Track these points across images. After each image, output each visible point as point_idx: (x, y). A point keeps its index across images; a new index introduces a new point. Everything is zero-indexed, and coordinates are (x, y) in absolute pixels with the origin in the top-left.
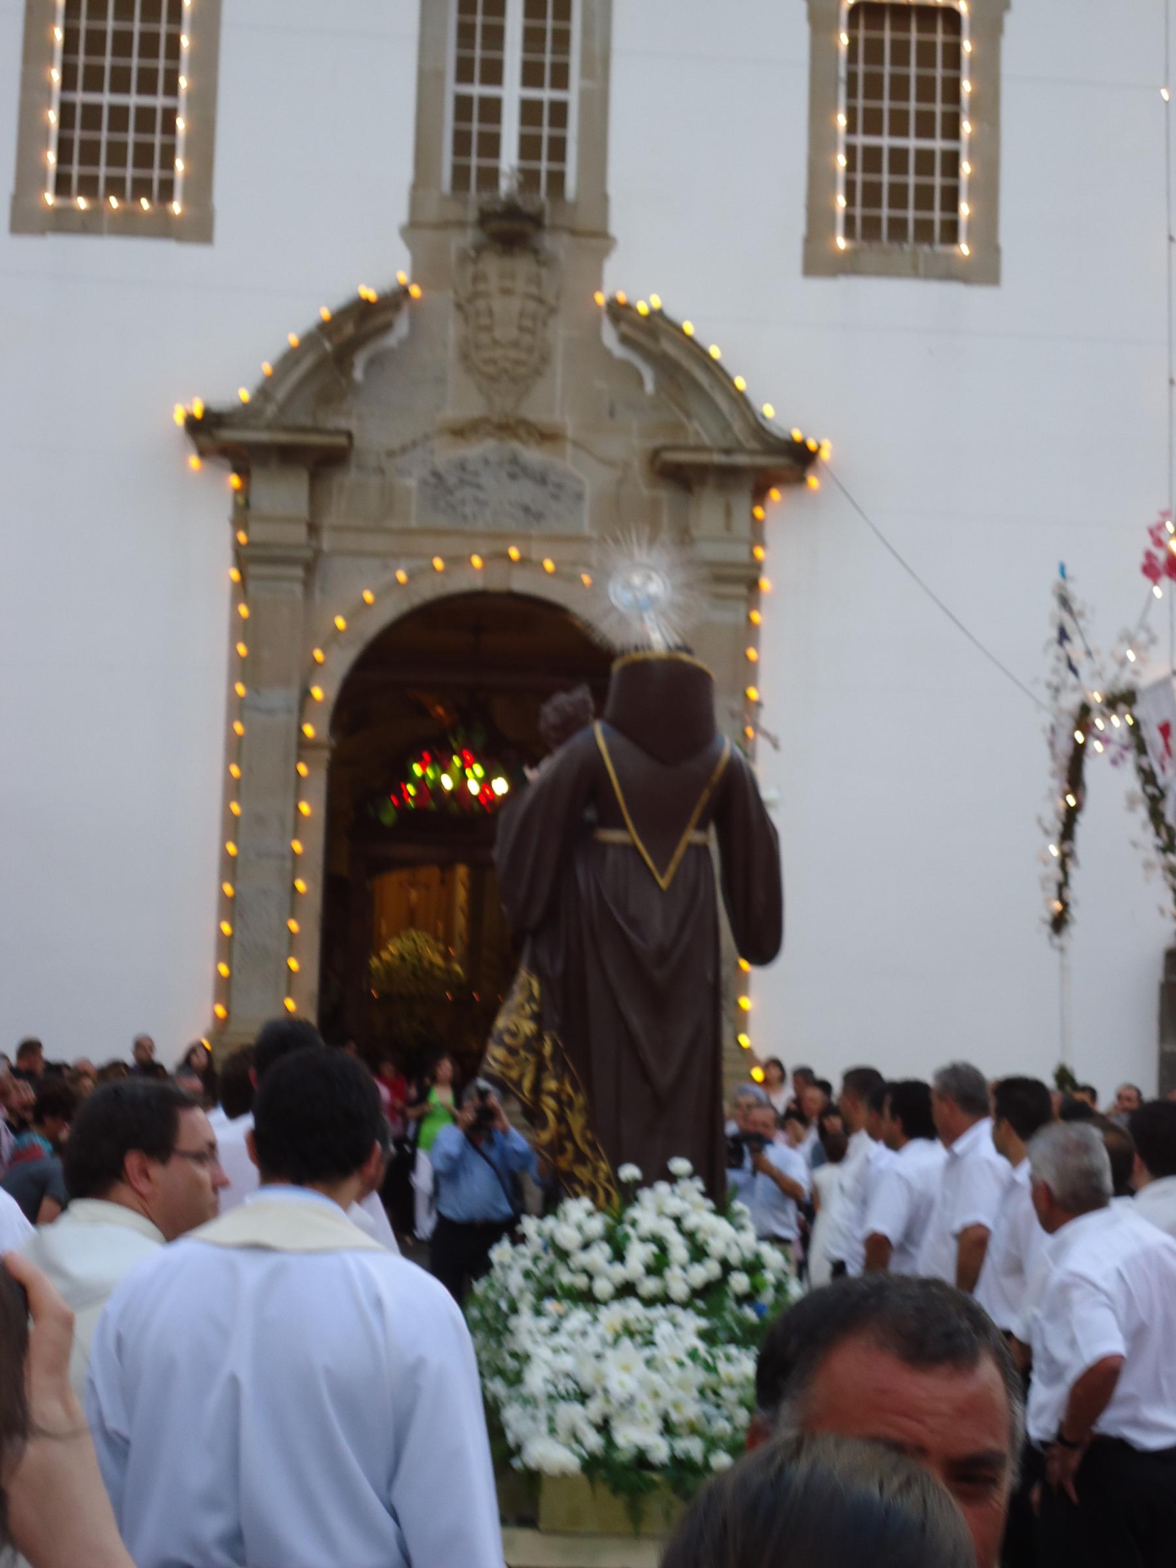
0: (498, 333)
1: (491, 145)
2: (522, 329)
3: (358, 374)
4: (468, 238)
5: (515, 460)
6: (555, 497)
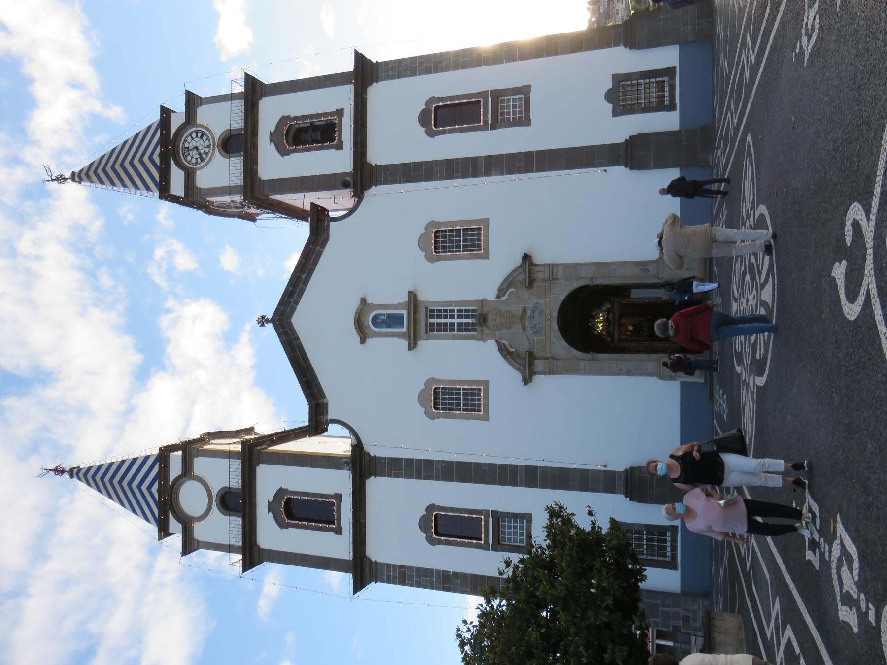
1: (467, 324)
2: (503, 317)
3: (514, 350)
4: (485, 328)
6: (537, 308)
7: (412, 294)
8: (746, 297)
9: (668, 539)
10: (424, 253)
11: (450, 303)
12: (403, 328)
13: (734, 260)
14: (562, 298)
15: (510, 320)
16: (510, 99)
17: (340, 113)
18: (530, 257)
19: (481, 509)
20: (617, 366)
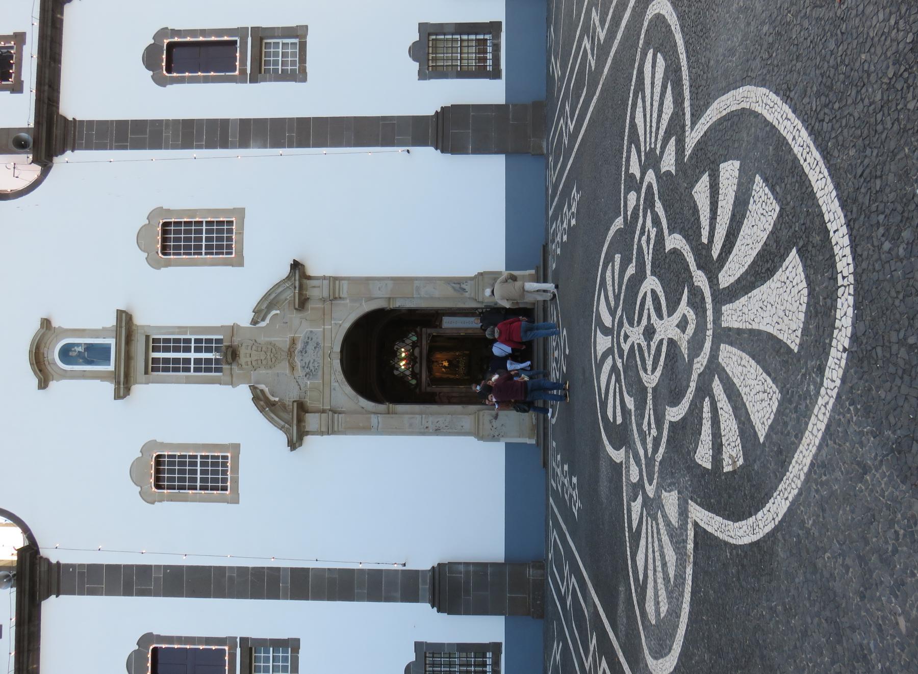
0: (263, 358)
1: (208, 361)
3: (277, 399)
6: (312, 339)
7: (124, 315)
8: (644, 322)
9: (489, 661)
10: (146, 255)
11: (183, 329)
12: (109, 365)
13: (601, 264)
14: (347, 325)
15: (272, 356)
16: (279, 43)
17: (20, 38)
18: (303, 266)
19: (224, 636)
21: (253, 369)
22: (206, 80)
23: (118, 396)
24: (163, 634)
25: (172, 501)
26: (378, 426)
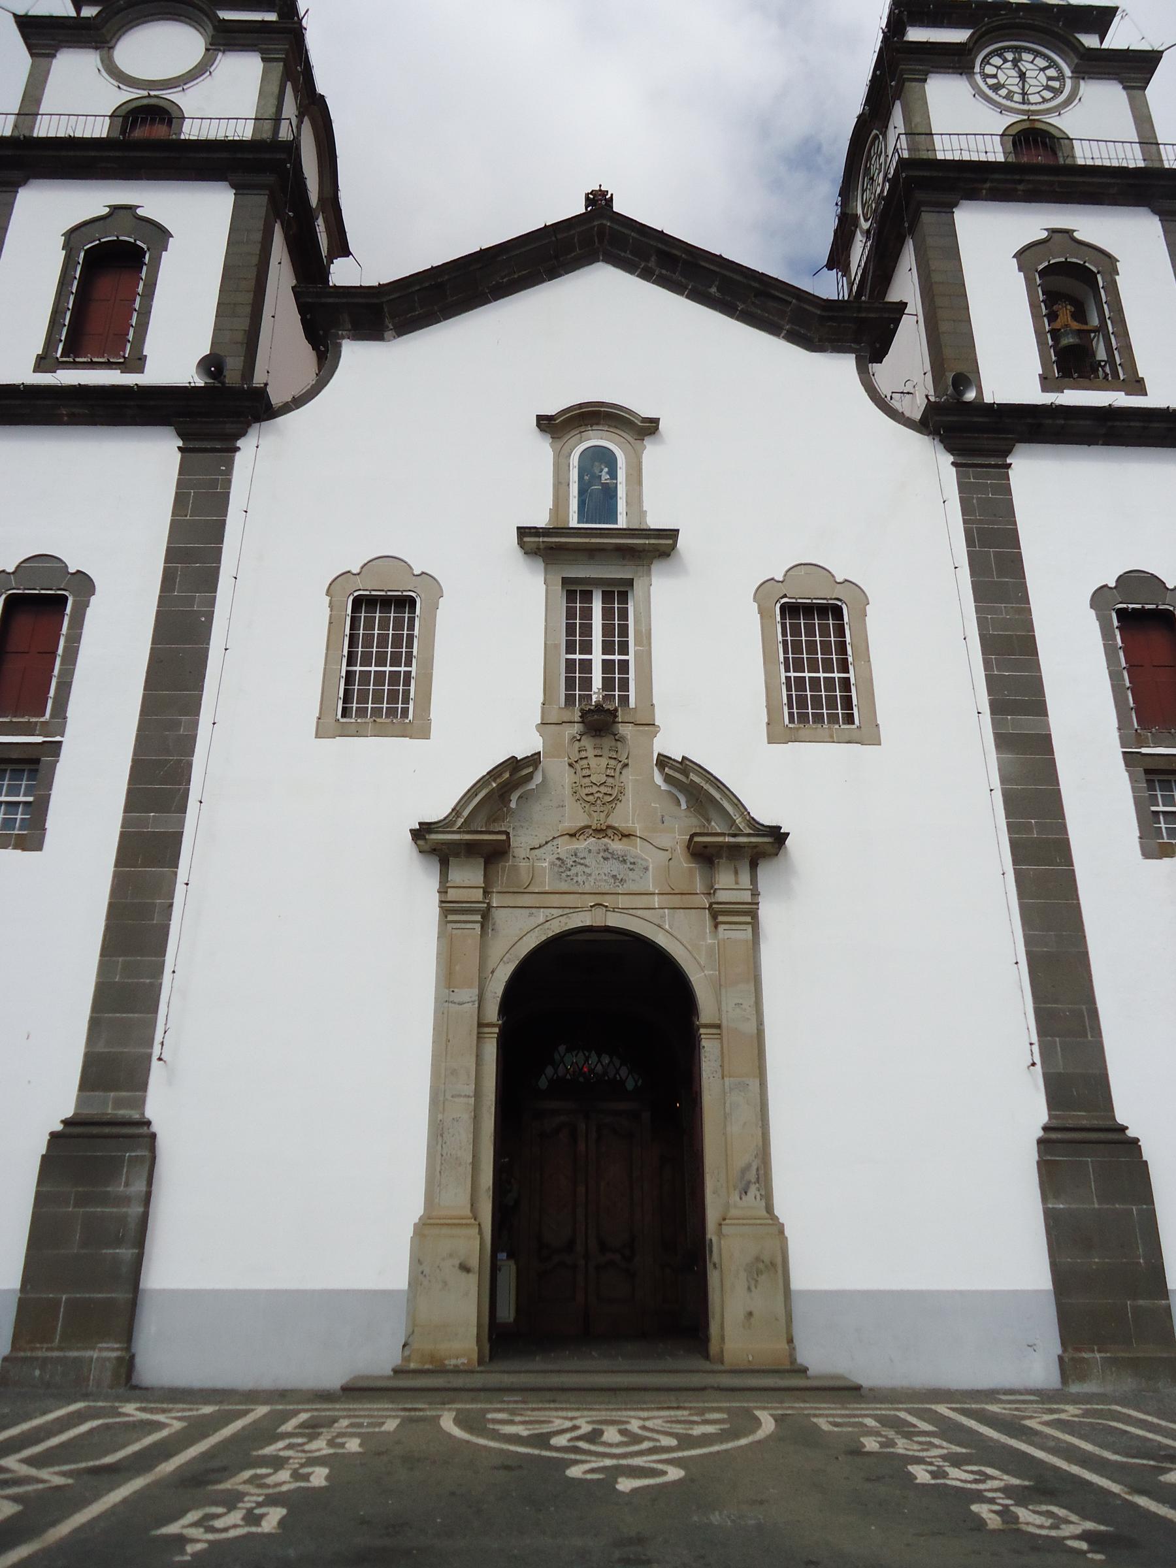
1: (587, 683)
2: (607, 776)
3: (513, 805)
4: (577, 728)
5: (606, 850)
11: (645, 638)
14: (661, 940)
17: (1137, 386)
19: (70, 713)
20: (460, 1096)
21: (572, 761)
22: (1114, 676)
23: (523, 532)
24: (89, 612)
25: (330, 623)
26: (455, 1003)
